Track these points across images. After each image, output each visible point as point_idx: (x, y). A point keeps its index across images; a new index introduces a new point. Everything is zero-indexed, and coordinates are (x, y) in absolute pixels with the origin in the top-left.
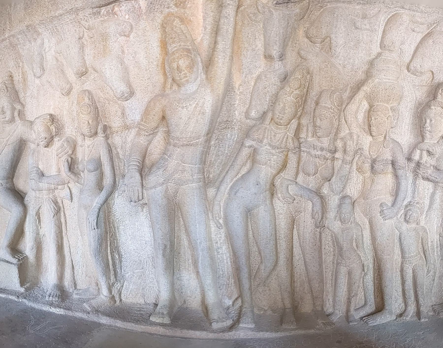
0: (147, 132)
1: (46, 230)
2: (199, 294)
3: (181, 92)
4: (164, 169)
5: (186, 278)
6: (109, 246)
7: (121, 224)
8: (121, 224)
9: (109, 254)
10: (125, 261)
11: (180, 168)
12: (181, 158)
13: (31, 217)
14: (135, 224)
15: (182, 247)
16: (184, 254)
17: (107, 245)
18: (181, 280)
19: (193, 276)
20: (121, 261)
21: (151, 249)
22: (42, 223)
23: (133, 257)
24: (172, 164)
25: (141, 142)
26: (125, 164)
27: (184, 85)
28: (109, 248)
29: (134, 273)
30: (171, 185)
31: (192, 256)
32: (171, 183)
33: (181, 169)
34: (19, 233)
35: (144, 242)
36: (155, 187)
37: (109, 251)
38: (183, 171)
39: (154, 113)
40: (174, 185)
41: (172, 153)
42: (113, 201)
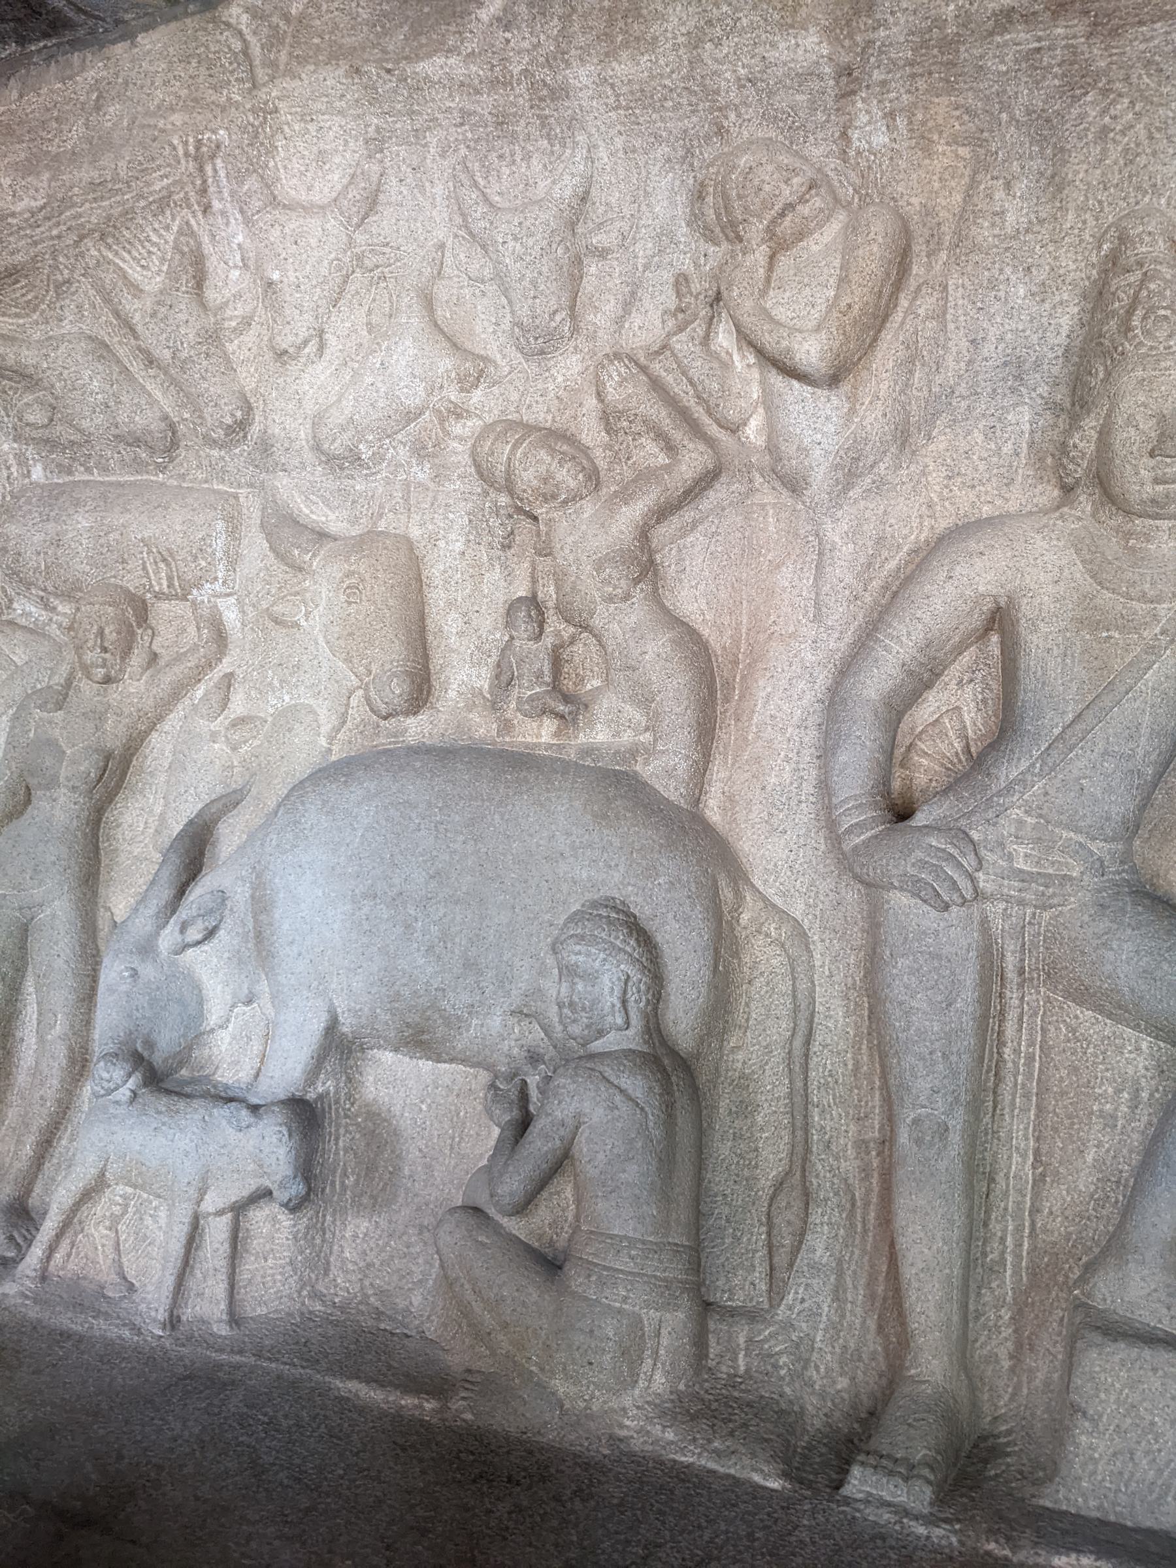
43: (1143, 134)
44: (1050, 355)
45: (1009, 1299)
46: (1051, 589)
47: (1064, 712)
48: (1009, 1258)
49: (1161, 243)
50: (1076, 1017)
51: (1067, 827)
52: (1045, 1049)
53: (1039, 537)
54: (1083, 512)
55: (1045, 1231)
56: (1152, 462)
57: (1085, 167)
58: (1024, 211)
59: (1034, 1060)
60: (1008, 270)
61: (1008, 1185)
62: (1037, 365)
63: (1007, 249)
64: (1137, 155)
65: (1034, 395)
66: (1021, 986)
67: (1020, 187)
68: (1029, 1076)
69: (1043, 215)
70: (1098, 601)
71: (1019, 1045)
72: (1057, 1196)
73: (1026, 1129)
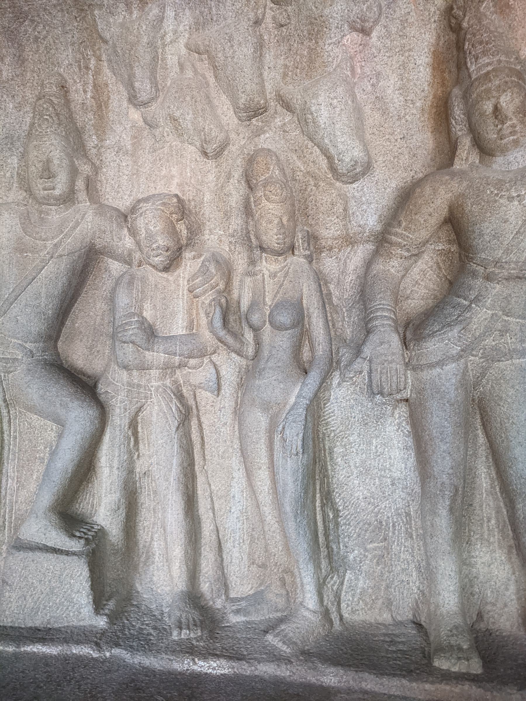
0: (408, 250)
1: (154, 460)
2: (514, 597)
3: (494, 166)
4: (462, 326)
5: (483, 560)
6: (318, 491)
7: (338, 444)
8: (338, 444)
9: (318, 509)
10: (345, 524)
11: (499, 325)
12: (503, 304)
13: (118, 433)
14: (371, 443)
15: (477, 492)
16: (481, 506)
17: (315, 489)
18: (470, 565)
19: (500, 555)
20: (337, 525)
21: (403, 495)
22: (141, 446)
23: (362, 514)
24: (480, 316)
25: (392, 270)
26: (344, 317)
27: (504, 151)
28: (318, 495)
29: (366, 550)
30: (474, 360)
31: (497, 512)
32: (475, 356)
33: (500, 328)
34: (84, 470)
35: (389, 480)
36: (440, 363)
37: (318, 504)
38: (503, 332)
39: (431, 210)
40: (482, 360)
41: (483, 293)
42: (327, 394)
43: (52, 42)
44: (23, 134)
45: (6, 541)
46: (7, 235)
47: (9, 288)
48: (7, 523)
49: (54, 88)
50: (31, 418)
51: (12, 337)
52: (20, 433)
53: (6, 213)
54: (28, 202)
55: (19, 510)
56: (41, 181)
57: (32, 53)
58: (10, 71)
59: (16, 438)
60: (5, 96)
61: (6, 493)
62: (19, 138)
63: (4, 87)
64: (51, 49)
65: (18, 151)
66: (7, 406)
67: (7, 60)
68: (15, 445)
69: (18, 73)
70: (23, 240)
71: (10, 433)
72: (23, 493)
73: (14, 468)
